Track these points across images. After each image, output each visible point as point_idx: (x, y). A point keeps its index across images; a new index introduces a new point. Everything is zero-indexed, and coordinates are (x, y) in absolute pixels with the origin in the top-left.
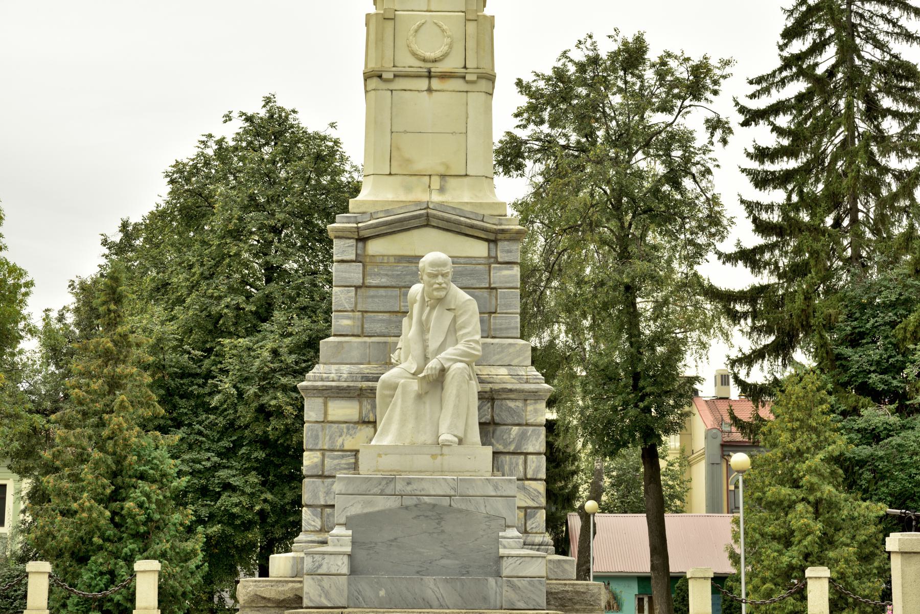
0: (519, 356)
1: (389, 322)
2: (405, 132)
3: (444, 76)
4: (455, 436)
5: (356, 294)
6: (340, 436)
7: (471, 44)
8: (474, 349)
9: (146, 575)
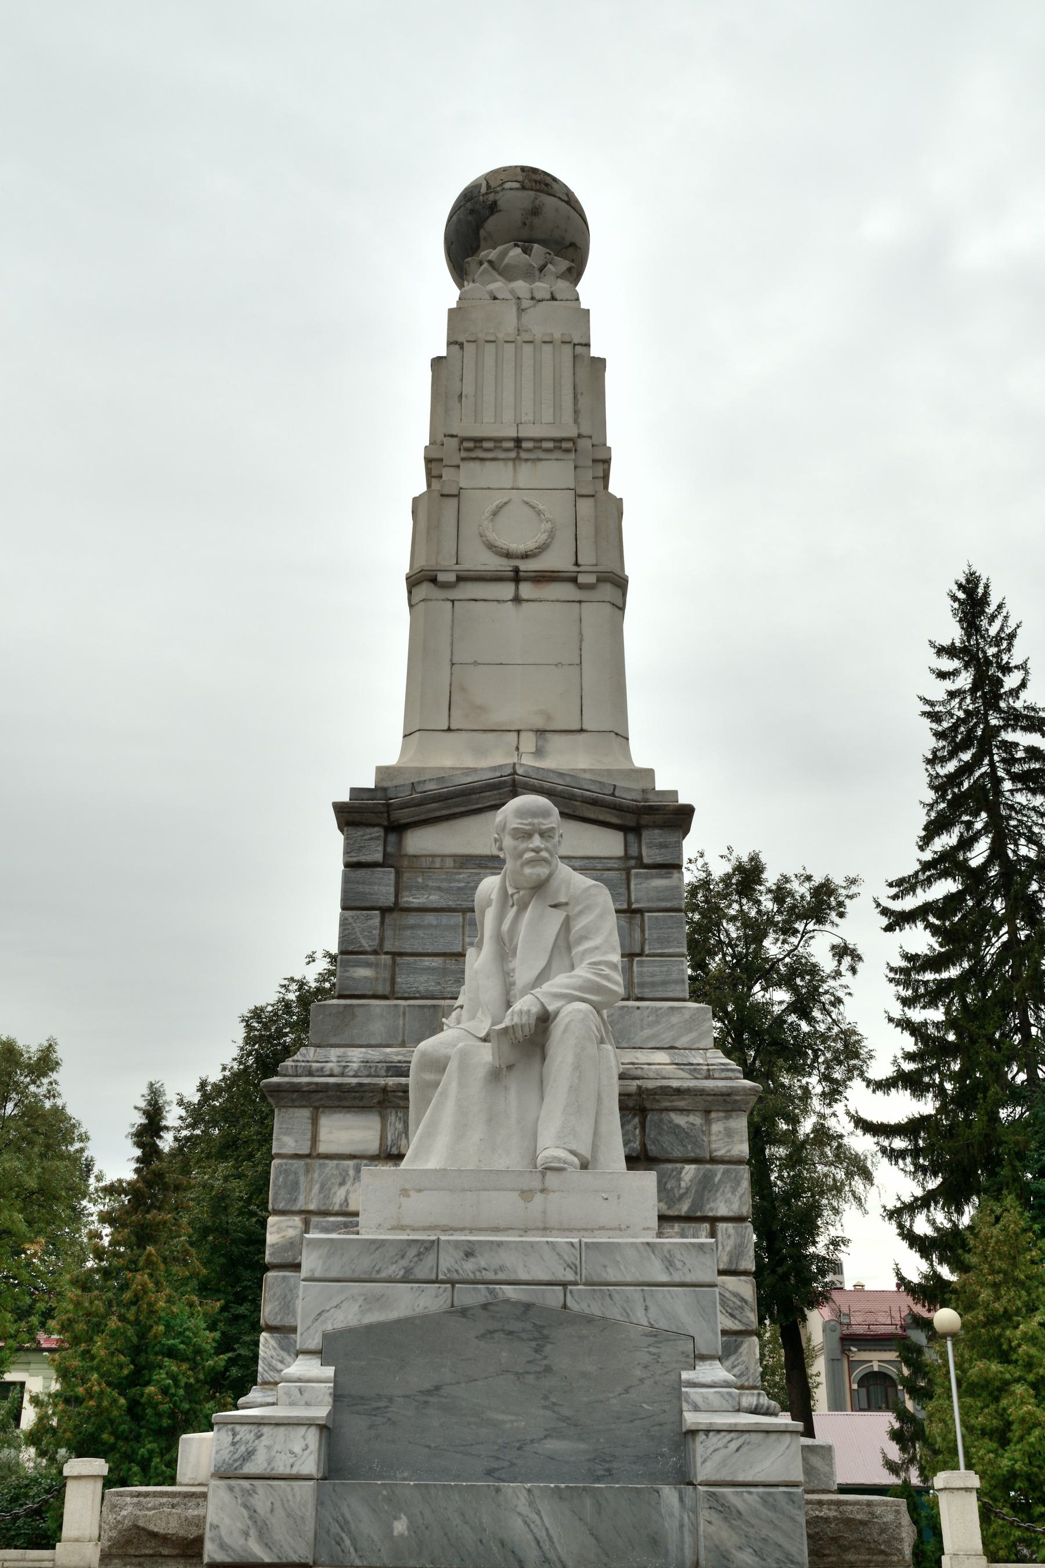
0: (690, 1030)
1: (444, 972)
2: (476, 663)
3: (543, 578)
4: (573, 1152)
5: (382, 923)
6: (342, 1184)
7: (586, 531)
8: (607, 977)
9: (83, 1483)
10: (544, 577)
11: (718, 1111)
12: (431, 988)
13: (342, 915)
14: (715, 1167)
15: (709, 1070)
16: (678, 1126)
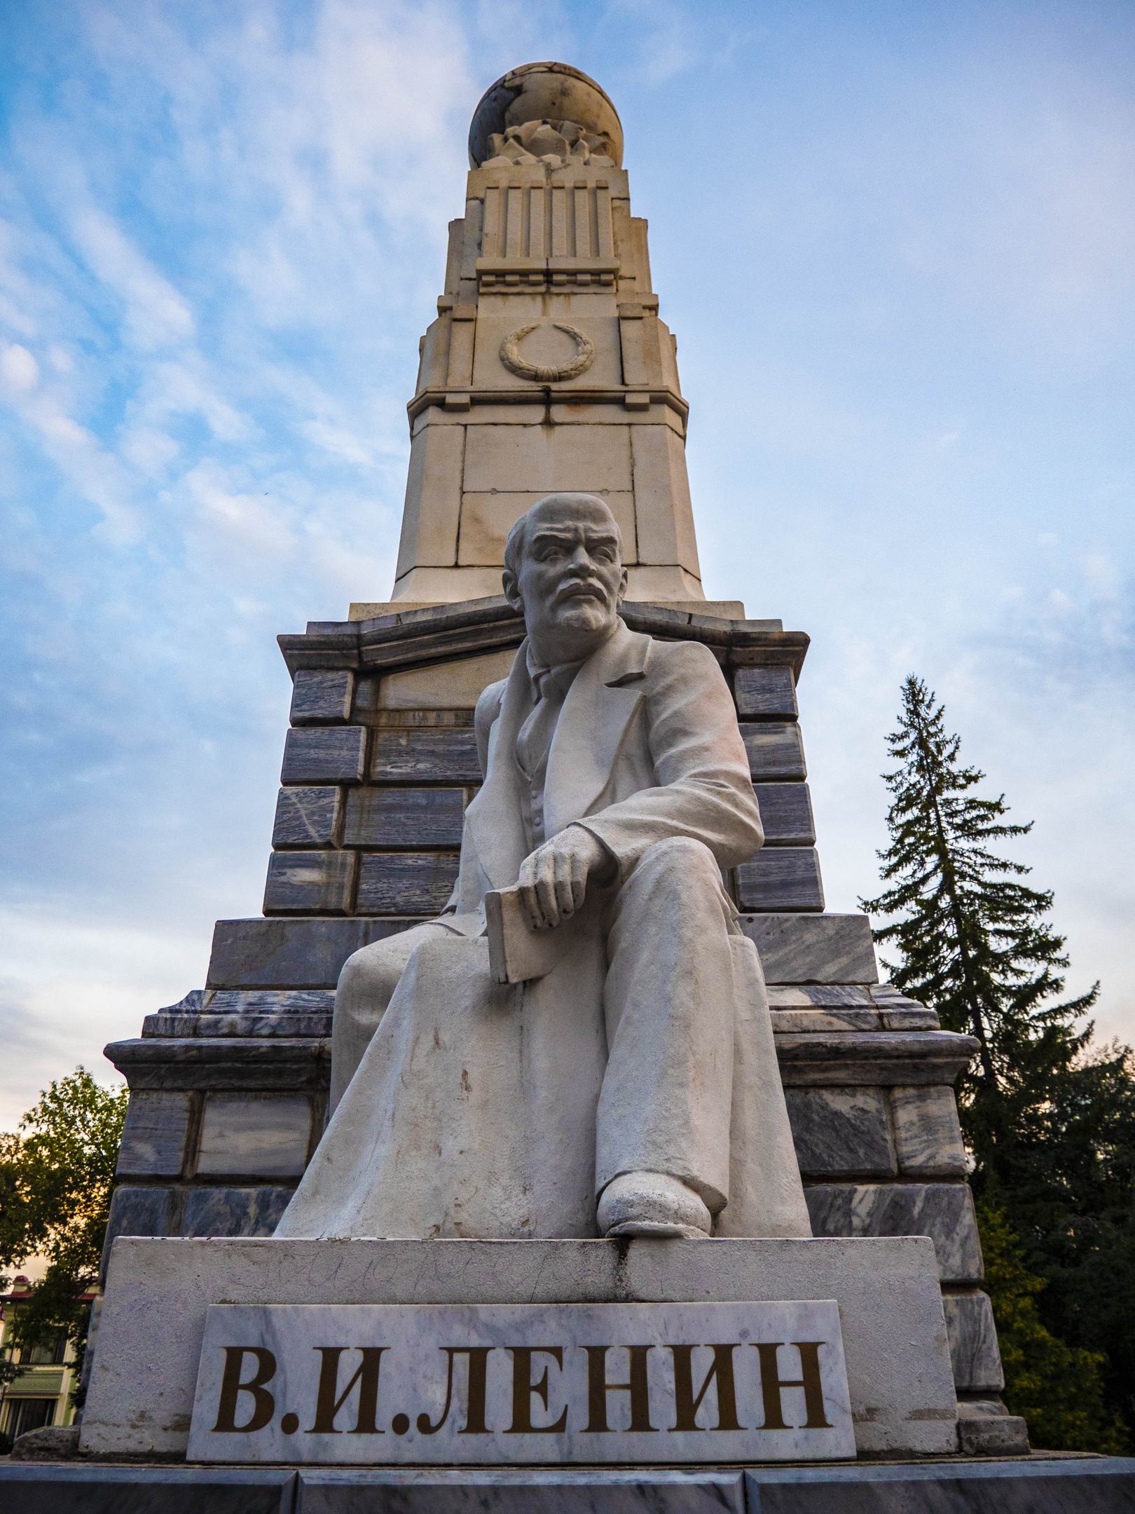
0: (837, 954)
4: (690, 1183)
10: (583, 398)
11: (904, 1086)
12: (415, 899)
13: (281, 793)
14: (910, 1186)
15: (881, 1016)
16: (837, 1114)
